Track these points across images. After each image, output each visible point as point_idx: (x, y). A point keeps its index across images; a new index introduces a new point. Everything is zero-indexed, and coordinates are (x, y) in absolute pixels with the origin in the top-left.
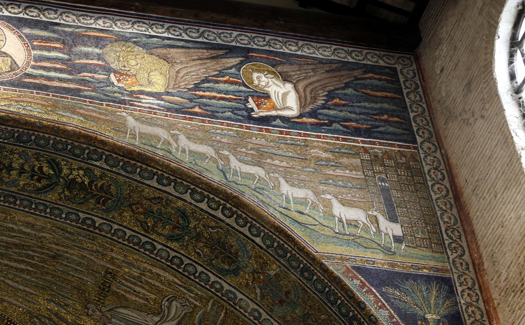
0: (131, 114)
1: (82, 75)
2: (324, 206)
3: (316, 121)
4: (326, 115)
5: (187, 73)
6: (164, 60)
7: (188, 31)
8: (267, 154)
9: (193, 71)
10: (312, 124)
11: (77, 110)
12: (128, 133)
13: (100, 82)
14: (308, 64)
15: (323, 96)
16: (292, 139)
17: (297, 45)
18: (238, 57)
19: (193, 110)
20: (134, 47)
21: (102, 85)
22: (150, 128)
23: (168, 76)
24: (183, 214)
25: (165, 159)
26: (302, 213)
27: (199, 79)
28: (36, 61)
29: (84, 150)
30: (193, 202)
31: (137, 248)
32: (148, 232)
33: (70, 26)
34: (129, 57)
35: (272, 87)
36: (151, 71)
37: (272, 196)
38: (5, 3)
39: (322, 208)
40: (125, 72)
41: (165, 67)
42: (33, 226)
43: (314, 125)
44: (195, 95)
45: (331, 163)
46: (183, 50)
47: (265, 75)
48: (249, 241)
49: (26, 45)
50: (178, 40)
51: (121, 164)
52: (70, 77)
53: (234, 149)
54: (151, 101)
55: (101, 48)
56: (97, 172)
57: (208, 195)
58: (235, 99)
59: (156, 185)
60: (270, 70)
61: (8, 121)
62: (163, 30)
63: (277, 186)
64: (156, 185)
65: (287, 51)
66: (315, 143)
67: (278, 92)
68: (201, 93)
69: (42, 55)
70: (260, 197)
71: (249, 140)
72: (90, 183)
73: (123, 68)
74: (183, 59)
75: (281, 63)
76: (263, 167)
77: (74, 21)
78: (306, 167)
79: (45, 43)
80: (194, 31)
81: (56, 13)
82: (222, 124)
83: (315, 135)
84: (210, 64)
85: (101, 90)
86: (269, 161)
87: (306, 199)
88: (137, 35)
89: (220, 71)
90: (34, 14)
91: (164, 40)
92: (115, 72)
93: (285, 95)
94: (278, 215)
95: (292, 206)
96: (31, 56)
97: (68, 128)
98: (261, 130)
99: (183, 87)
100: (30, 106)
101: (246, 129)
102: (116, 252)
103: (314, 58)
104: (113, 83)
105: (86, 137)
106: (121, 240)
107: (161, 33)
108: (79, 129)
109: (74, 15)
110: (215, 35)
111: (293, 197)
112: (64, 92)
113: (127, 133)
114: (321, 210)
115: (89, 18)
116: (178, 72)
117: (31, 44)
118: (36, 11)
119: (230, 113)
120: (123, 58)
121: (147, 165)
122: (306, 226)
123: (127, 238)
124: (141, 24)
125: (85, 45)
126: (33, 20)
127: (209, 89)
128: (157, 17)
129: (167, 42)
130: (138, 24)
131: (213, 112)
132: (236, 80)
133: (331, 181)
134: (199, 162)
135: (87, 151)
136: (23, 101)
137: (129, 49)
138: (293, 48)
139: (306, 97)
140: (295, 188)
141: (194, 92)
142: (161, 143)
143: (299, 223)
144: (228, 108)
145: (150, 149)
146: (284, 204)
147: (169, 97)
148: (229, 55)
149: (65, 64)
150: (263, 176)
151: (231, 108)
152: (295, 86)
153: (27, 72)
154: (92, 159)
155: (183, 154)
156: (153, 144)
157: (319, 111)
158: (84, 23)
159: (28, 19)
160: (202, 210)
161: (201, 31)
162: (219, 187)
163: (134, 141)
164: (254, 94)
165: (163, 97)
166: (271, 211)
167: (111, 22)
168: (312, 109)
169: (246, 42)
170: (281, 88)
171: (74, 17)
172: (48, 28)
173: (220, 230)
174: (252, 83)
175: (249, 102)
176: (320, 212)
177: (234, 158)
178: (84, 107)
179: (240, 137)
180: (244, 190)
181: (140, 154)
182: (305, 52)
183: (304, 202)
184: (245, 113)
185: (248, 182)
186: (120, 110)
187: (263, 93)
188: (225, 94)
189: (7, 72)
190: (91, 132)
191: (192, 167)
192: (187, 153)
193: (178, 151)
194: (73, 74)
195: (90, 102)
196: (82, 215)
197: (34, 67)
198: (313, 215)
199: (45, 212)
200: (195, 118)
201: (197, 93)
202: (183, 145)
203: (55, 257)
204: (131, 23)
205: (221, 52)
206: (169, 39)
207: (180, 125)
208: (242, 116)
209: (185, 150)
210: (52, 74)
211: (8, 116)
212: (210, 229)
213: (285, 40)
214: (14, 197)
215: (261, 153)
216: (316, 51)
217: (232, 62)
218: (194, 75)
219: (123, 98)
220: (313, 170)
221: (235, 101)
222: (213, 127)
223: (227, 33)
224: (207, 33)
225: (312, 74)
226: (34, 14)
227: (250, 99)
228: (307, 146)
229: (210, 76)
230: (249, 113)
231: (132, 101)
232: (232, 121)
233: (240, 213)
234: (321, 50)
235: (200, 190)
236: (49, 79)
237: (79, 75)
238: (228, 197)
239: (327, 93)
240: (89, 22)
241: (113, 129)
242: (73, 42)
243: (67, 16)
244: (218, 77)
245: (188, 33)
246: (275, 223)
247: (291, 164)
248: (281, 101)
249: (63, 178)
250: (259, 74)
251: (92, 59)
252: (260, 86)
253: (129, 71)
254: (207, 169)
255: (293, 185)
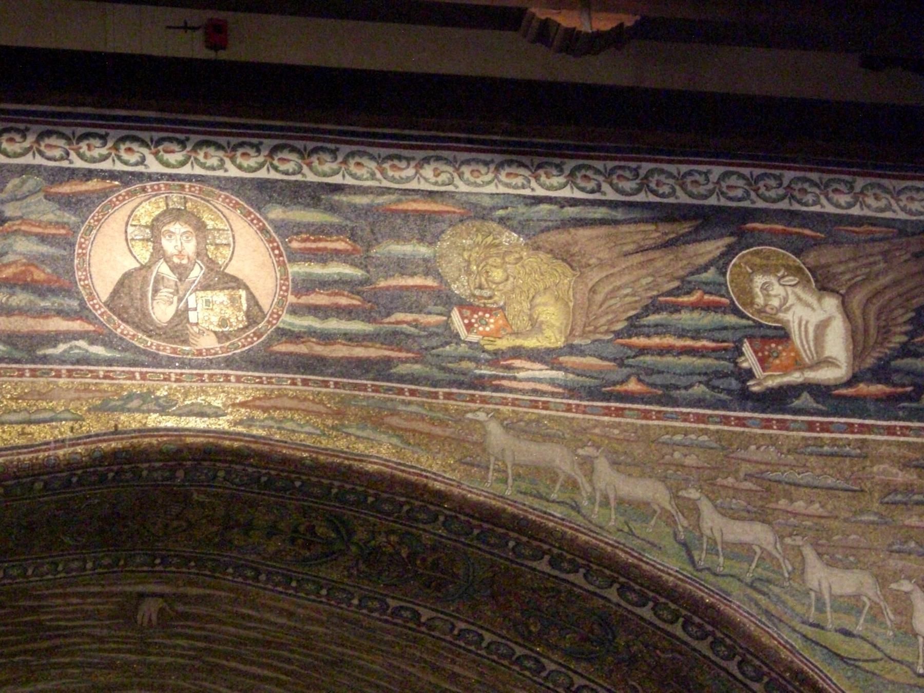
0: (496, 415)
1: (392, 318)
2: (897, 612)
3: (887, 389)
4: (908, 373)
5: (613, 291)
6: (564, 260)
7: (615, 177)
8: (780, 487)
9: (625, 286)
10: (877, 399)
11: (387, 420)
12: (491, 467)
13: (431, 335)
14: (873, 240)
15: (905, 323)
16: (834, 442)
17: (852, 188)
18: (722, 236)
19: (624, 387)
20: (500, 234)
21: (434, 341)
22: (534, 447)
23: (571, 304)
24: (605, 622)
25: (566, 526)
26: (847, 633)
27: (637, 305)
28: (297, 293)
29: (401, 506)
30: (623, 603)
31: (506, 662)
32: (529, 640)
33: (364, 191)
34: (491, 261)
35: (794, 308)
36: (537, 293)
37: (788, 597)
38: (229, 143)
39: (892, 617)
40: (480, 303)
41: (565, 278)
42: (291, 614)
43: (882, 400)
44: (630, 347)
45: (916, 497)
46: (603, 230)
47: (780, 279)
48: (738, 684)
49: (277, 252)
50: (593, 203)
51: (476, 532)
52: (368, 328)
53: (711, 487)
54: (537, 374)
55: (431, 244)
56: (427, 539)
57: (655, 598)
58: (714, 350)
59: (548, 569)
60: (791, 263)
61: (248, 456)
62: (562, 180)
63: (800, 571)
64: (548, 569)
65: (830, 209)
66: (882, 449)
67: (807, 322)
68: (642, 341)
69: (310, 274)
70: (763, 601)
71: (742, 454)
72: (412, 556)
73: (477, 292)
74: (605, 255)
75: (816, 243)
76: (770, 523)
77: (373, 175)
78: (862, 512)
79: (314, 241)
80: (627, 174)
81: (336, 158)
82: (685, 417)
83: (883, 427)
84: (662, 261)
85: (433, 355)
86: (783, 503)
87: (857, 597)
88: (508, 200)
89: (682, 279)
90: (290, 166)
91: (562, 207)
92: (462, 304)
93: (822, 327)
94: (798, 644)
95: (831, 620)
96: (287, 279)
97: (370, 467)
98: (767, 424)
99: (603, 329)
100: (292, 419)
101: (736, 425)
102: (461, 666)
103: (888, 223)
104: (457, 335)
105: (406, 484)
106: (472, 648)
107: (556, 189)
108: (392, 468)
109: (372, 158)
110: (671, 181)
111: (831, 595)
112: (358, 372)
113: (488, 468)
114: (889, 623)
115: (403, 164)
116: (593, 291)
117: (287, 248)
118: (294, 157)
119: (703, 388)
120: (478, 266)
121: (530, 537)
122: (857, 663)
123: (484, 645)
124: (513, 170)
125: (399, 238)
126: (288, 182)
127: (660, 329)
128: (548, 146)
129: (570, 211)
130: (508, 170)
131: (666, 387)
132: (717, 299)
133: (912, 545)
134: (636, 527)
135: (406, 508)
136: (276, 408)
137: (489, 240)
138: (843, 199)
139: (866, 331)
140: (836, 571)
141: (627, 341)
142: (558, 487)
143: (842, 658)
144: (699, 374)
145: (536, 504)
146: (813, 616)
147: (573, 359)
148: (703, 233)
149: (358, 293)
150: (770, 548)
151: (706, 374)
152: (843, 303)
153: (281, 326)
154: (417, 520)
155: (603, 511)
156: (543, 490)
157: (893, 363)
158: (393, 179)
159: (277, 181)
160: (642, 618)
161: (642, 172)
162: (676, 586)
163: (503, 487)
164: (756, 332)
165: (561, 359)
166: (786, 635)
167: (450, 169)
168: (880, 359)
169: (739, 193)
170: (813, 309)
171: (373, 165)
172: (319, 200)
173: (679, 656)
174: (752, 303)
175: (742, 354)
176: (886, 628)
177: (710, 504)
178: (401, 407)
179: (723, 448)
180: (729, 589)
181: (514, 517)
182: (869, 207)
183: (852, 604)
184: (734, 384)
185: (737, 568)
186: (472, 405)
187: (775, 328)
188: (693, 338)
189: (242, 329)
190: (415, 474)
191: (623, 541)
192: (613, 504)
193: (593, 504)
194: (375, 321)
195: (413, 393)
196: (393, 603)
197: (295, 310)
198: (870, 636)
199: (318, 594)
200: (630, 409)
201: (635, 340)
202: (603, 487)
203: (337, 663)
204: (492, 167)
205: (684, 228)
206: (574, 202)
207: (597, 431)
208: (729, 392)
209: (606, 497)
210: (334, 324)
211: (248, 448)
212: (658, 652)
213: (826, 177)
214: (255, 569)
215: (766, 484)
216: (893, 201)
217: (710, 252)
218: (627, 295)
219: (478, 372)
220: (876, 519)
221: (714, 354)
222: (666, 427)
223: (700, 173)
224: (656, 177)
225: (882, 265)
226: (290, 166)
227: (746, 348)
228: (865, 457)
229: (662, 295)
230: (744, 382)
231: (497, 377)
232: (708, 407)
233: (719, 635)
234: (903, 197)
235: (637, 587)
236: (327, 338)
237: (387, 320)
238: (695, 605)
239: (913, 314)
240: (404, 174)
241: (460, 461)
242: (372, 231)
243: (358, 164)
244: (678, 296)
245: (615, 181)
246: (792, 662)
247: (829, 507)
248: (812, 344)
249: (357, 544)
250: (766, 279)
251: (412, 275)
252: (768, 309)
253: (490, 297)
254: (653, 545)
255: (832, 563)
